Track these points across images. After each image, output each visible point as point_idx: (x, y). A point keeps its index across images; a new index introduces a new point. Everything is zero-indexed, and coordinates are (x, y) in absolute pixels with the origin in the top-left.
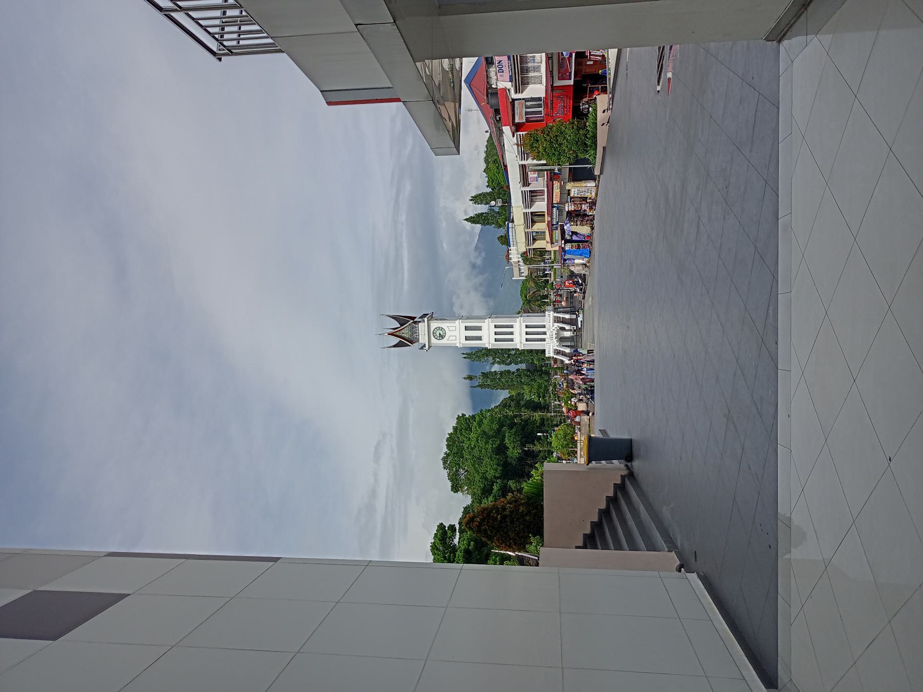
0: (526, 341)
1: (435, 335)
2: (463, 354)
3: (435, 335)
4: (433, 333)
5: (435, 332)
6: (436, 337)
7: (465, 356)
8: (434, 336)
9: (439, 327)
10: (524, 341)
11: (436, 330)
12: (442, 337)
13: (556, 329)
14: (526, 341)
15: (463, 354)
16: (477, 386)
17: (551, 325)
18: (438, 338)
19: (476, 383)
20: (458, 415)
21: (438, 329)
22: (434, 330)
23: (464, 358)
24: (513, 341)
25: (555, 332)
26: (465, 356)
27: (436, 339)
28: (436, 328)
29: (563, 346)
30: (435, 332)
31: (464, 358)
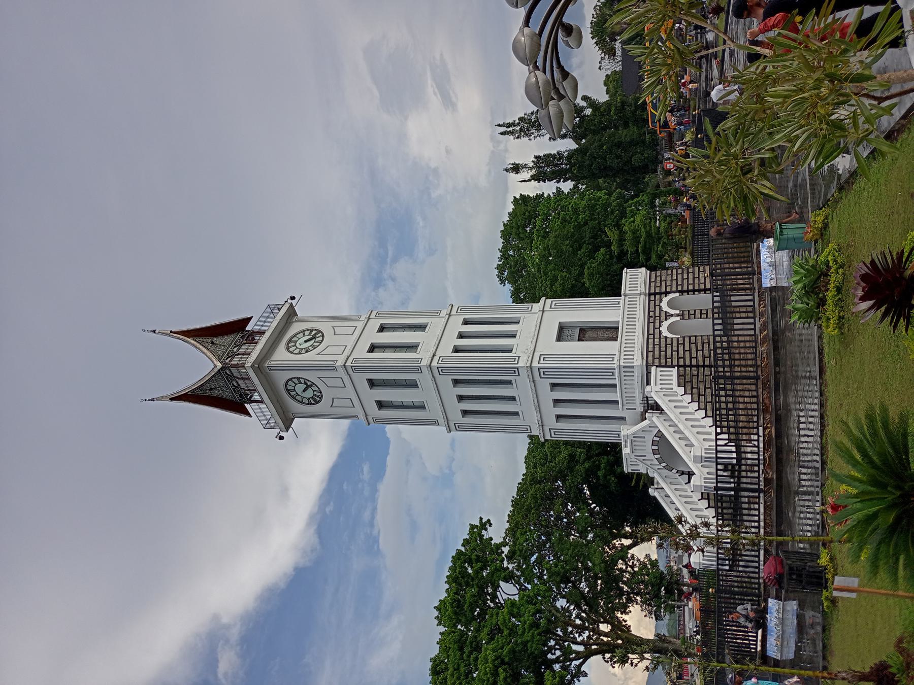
2: (499, 125)
3: (293, 393)
4: (288, 391)
6: (299, 398)
7: (503, 129)
8: (293, 397)
10: (551, 422)
12: (316, 399)
15: (499, 125)
16: (529, 180)
19: (526, 175)
20: (515, 197)
21: (296, 381)
23: (502, 134)
26: (503, 129)
27: (302, 402)
28: (290, 379)
30: (289, 387)
31: (502, 134)
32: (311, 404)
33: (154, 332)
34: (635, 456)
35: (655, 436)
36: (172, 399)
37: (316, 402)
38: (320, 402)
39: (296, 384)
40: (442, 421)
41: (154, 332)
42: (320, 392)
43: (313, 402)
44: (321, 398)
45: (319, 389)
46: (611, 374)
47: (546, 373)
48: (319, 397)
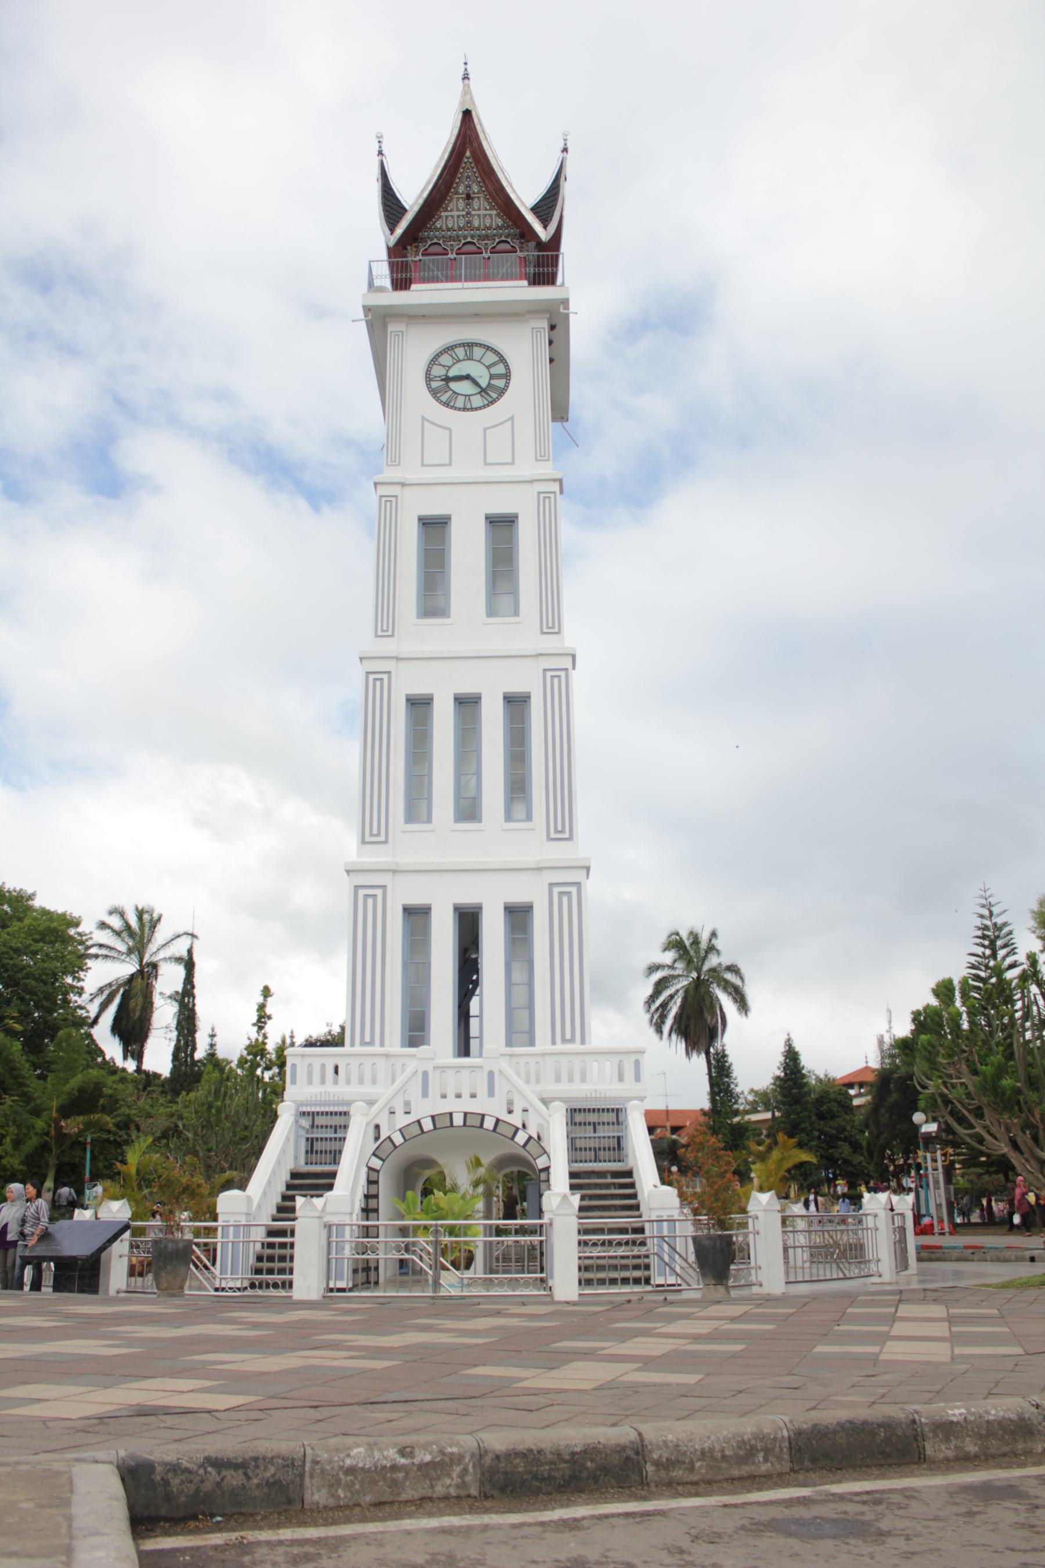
0: (409, 911)
1: (460, 352)
4: (470, 345)
5: (478, 352)
8: (449, 349)
9: (507, 376)
11: (491, 358)
13: (516, 1120)
14: (409, 911)
17: (551, 1088)
18: (438, 371)
21: (500, 369)
22: (488, 348)
24: (412, 815)
25: (493, 1108)
27: (434, 361)
28: (502, 360)
29: (372, 1182)
30: (478, 352)
32: (429, 378)
33: (565, 150)
34: (425, 1074)
35: (498, 1121)
36: (467, 114)
37: (435, 393)
38: (438, 400)
39: (488, 367)
40: (388, 647)
41: (565, 150)
42: (465, 409)
43: (434, 385)
44: (446, 404)
45: (476, 409)
46: (568, 1036)
47: (565, 899)
48: (450, 399)
